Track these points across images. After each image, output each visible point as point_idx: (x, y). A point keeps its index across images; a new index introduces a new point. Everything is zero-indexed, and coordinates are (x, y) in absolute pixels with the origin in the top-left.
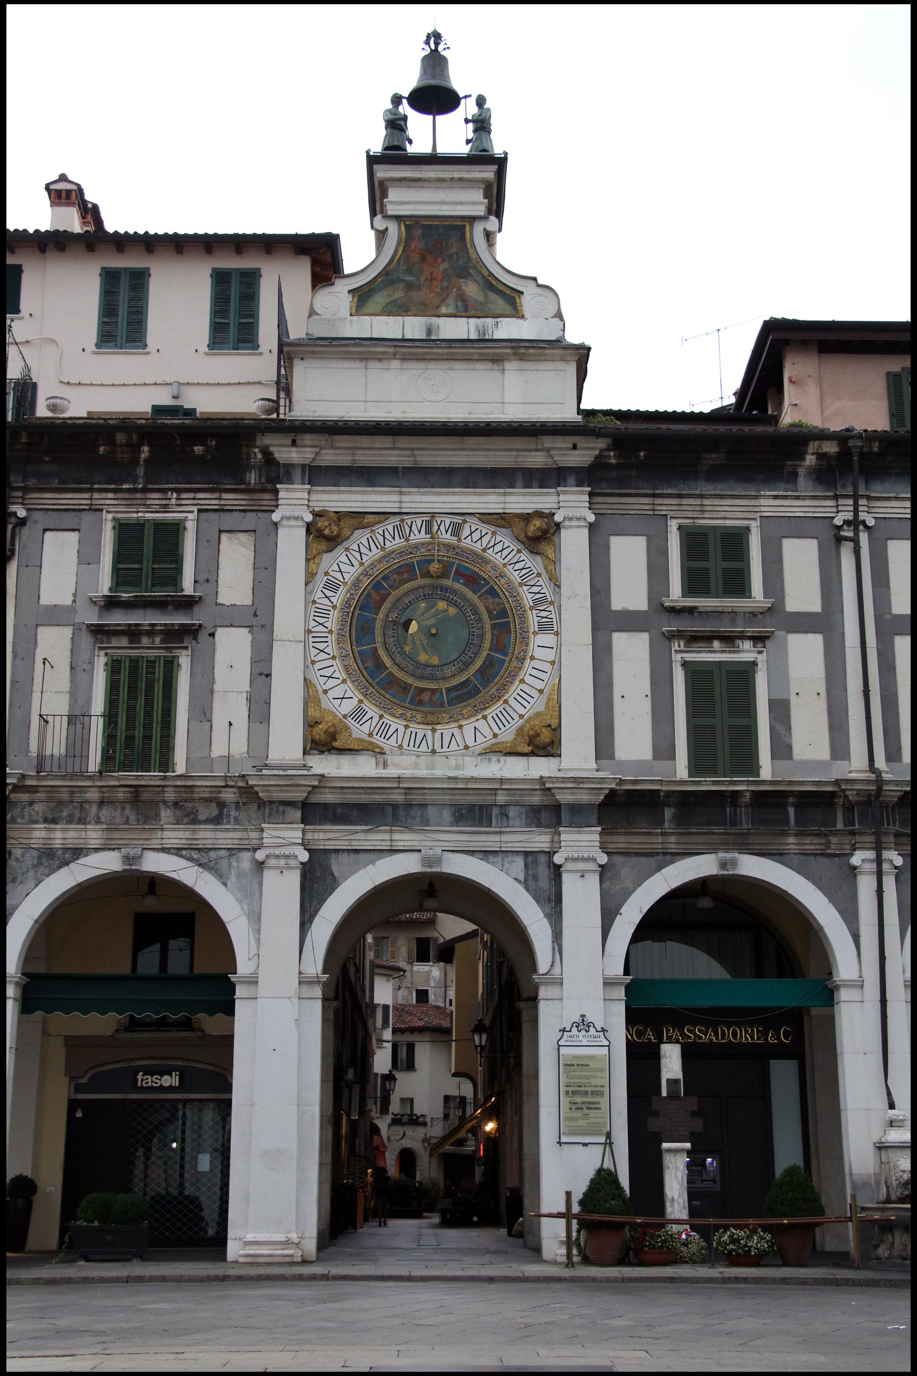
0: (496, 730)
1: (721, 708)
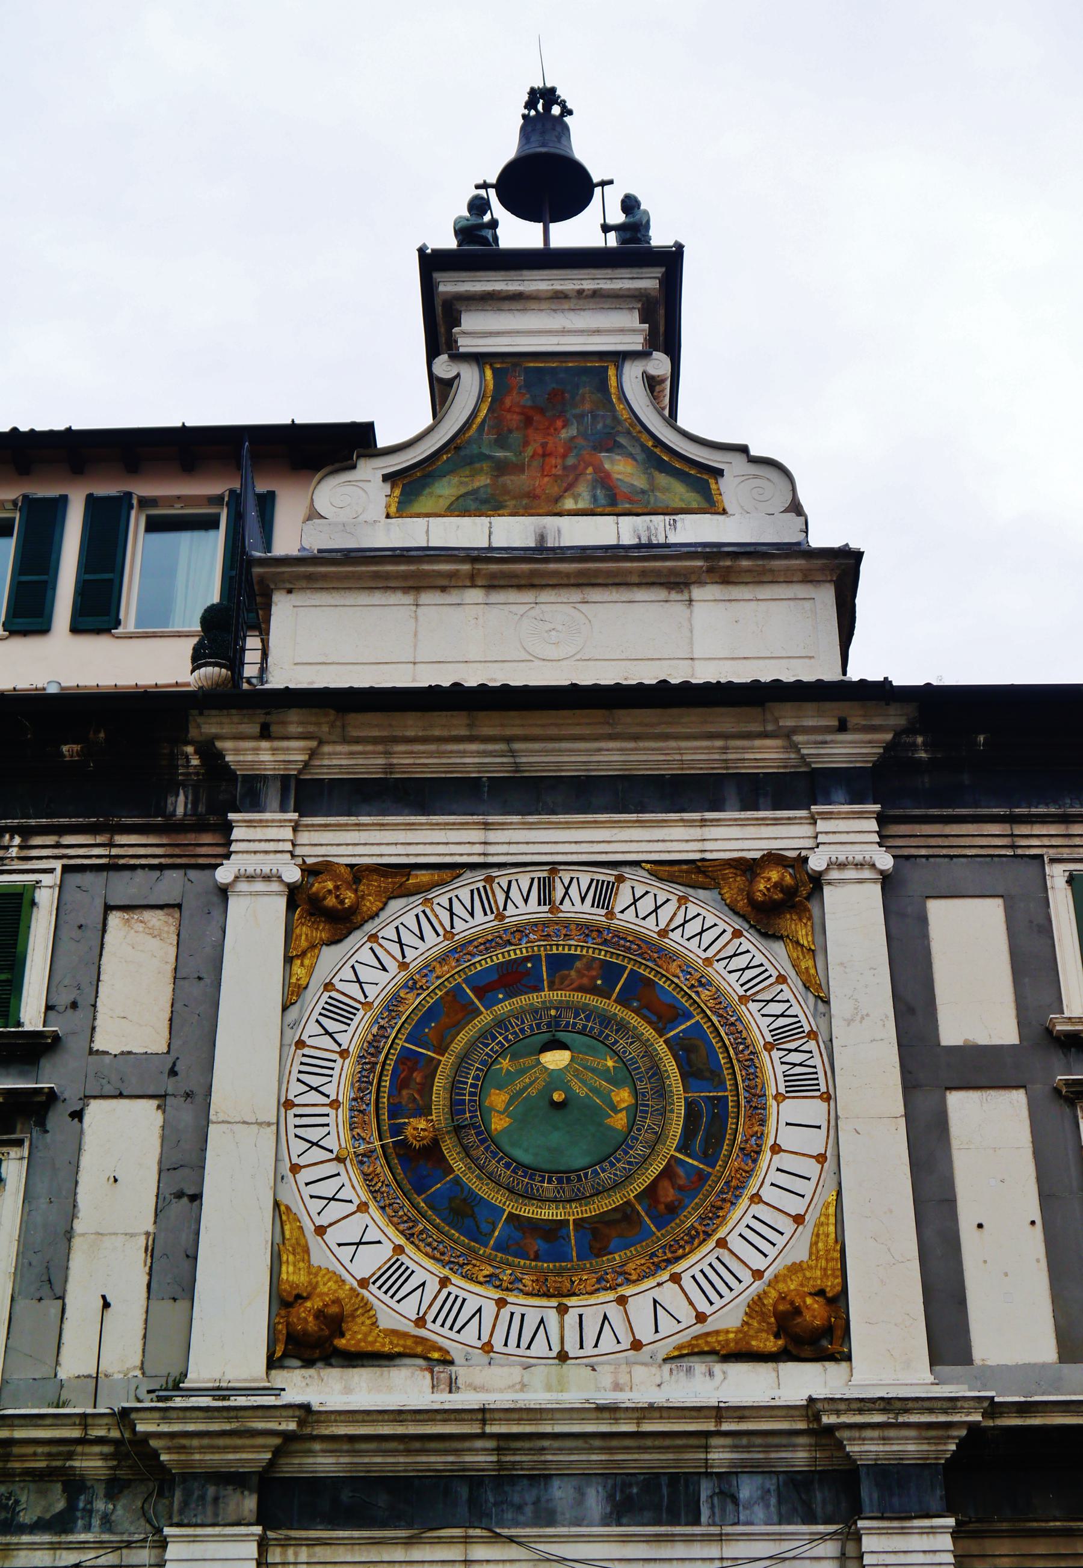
0: (703, 1306)
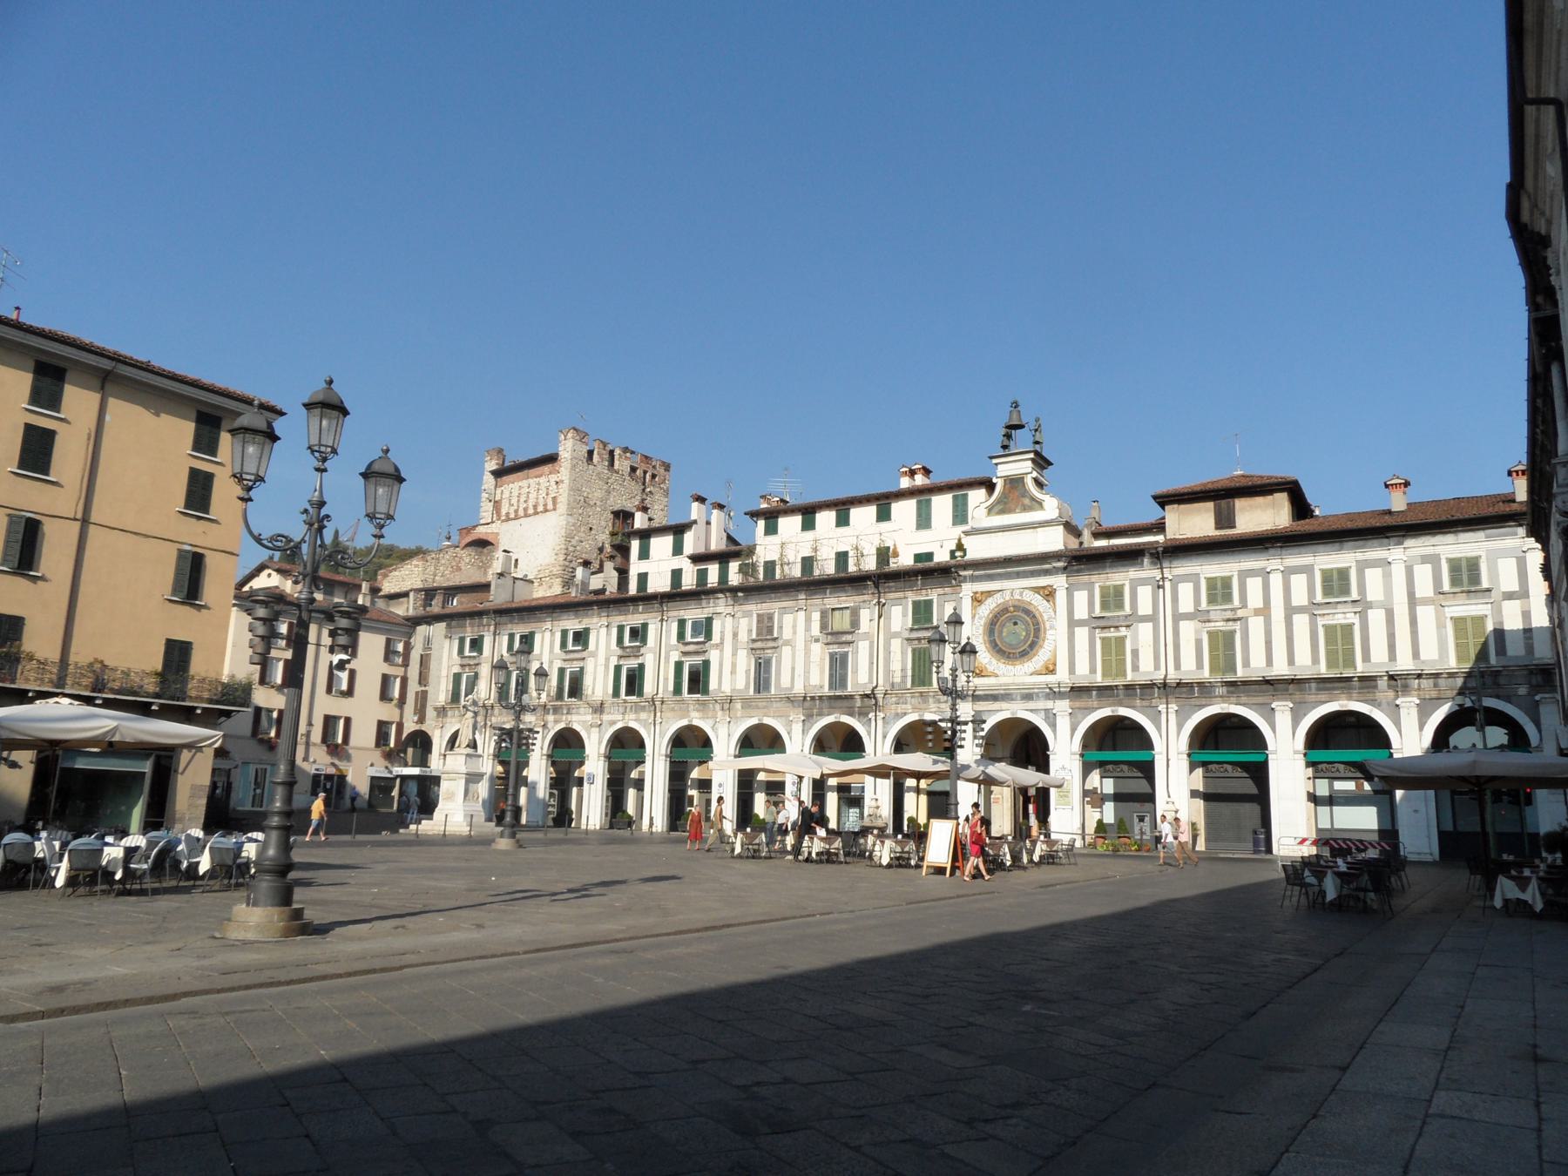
1: (1114, 652)
